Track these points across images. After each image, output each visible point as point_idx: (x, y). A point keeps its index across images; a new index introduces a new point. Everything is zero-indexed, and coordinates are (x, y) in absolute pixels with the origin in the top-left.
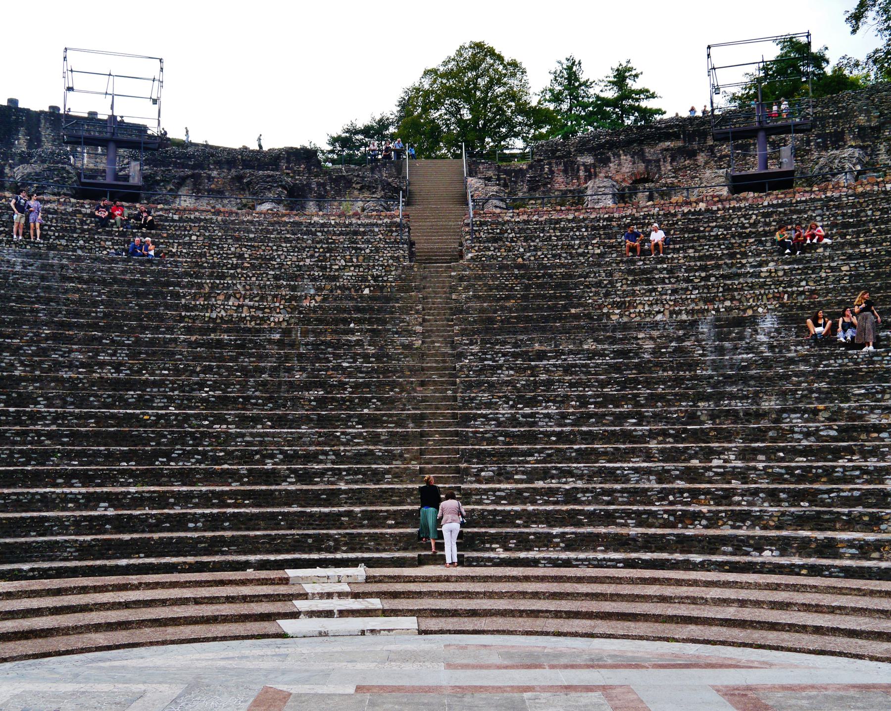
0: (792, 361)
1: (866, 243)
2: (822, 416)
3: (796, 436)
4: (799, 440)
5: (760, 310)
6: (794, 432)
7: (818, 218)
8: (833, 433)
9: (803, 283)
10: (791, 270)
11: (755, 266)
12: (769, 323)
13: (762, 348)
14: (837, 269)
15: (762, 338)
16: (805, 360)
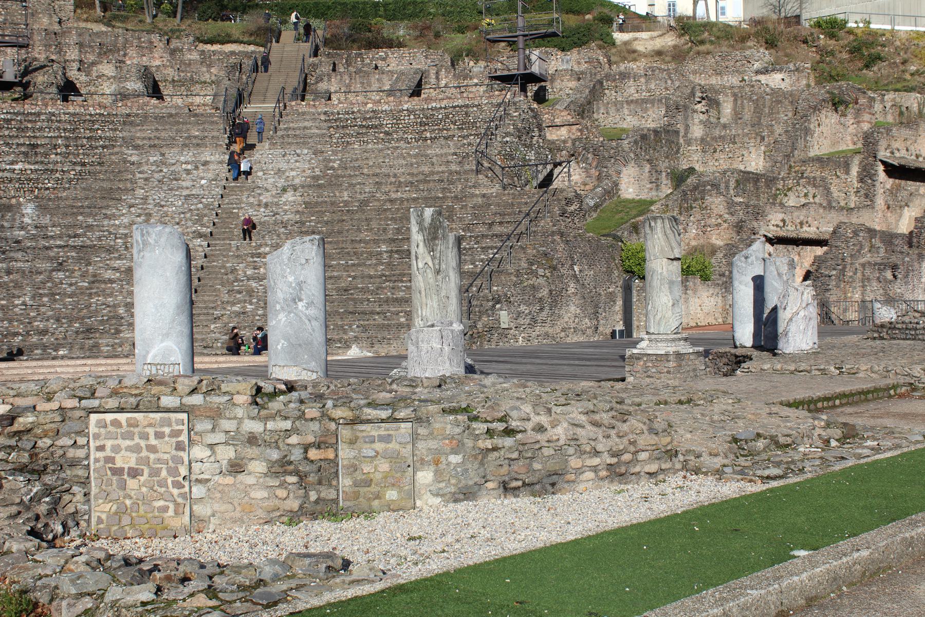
0: (52, 237)
1: (84, 154)
2: (77, 274)
3: (64, 286)
4: (65, 289)
5: (21, 199)
6: (62, 284)
7: (47, 130)
8: (86, 284)
9: (46, 181)
10: (36, 170)
11: (9, 164)
12: (29, 209)
13: (29, 228)
14: (68, 171)
15: (27, 220)
16: (60, 237)
